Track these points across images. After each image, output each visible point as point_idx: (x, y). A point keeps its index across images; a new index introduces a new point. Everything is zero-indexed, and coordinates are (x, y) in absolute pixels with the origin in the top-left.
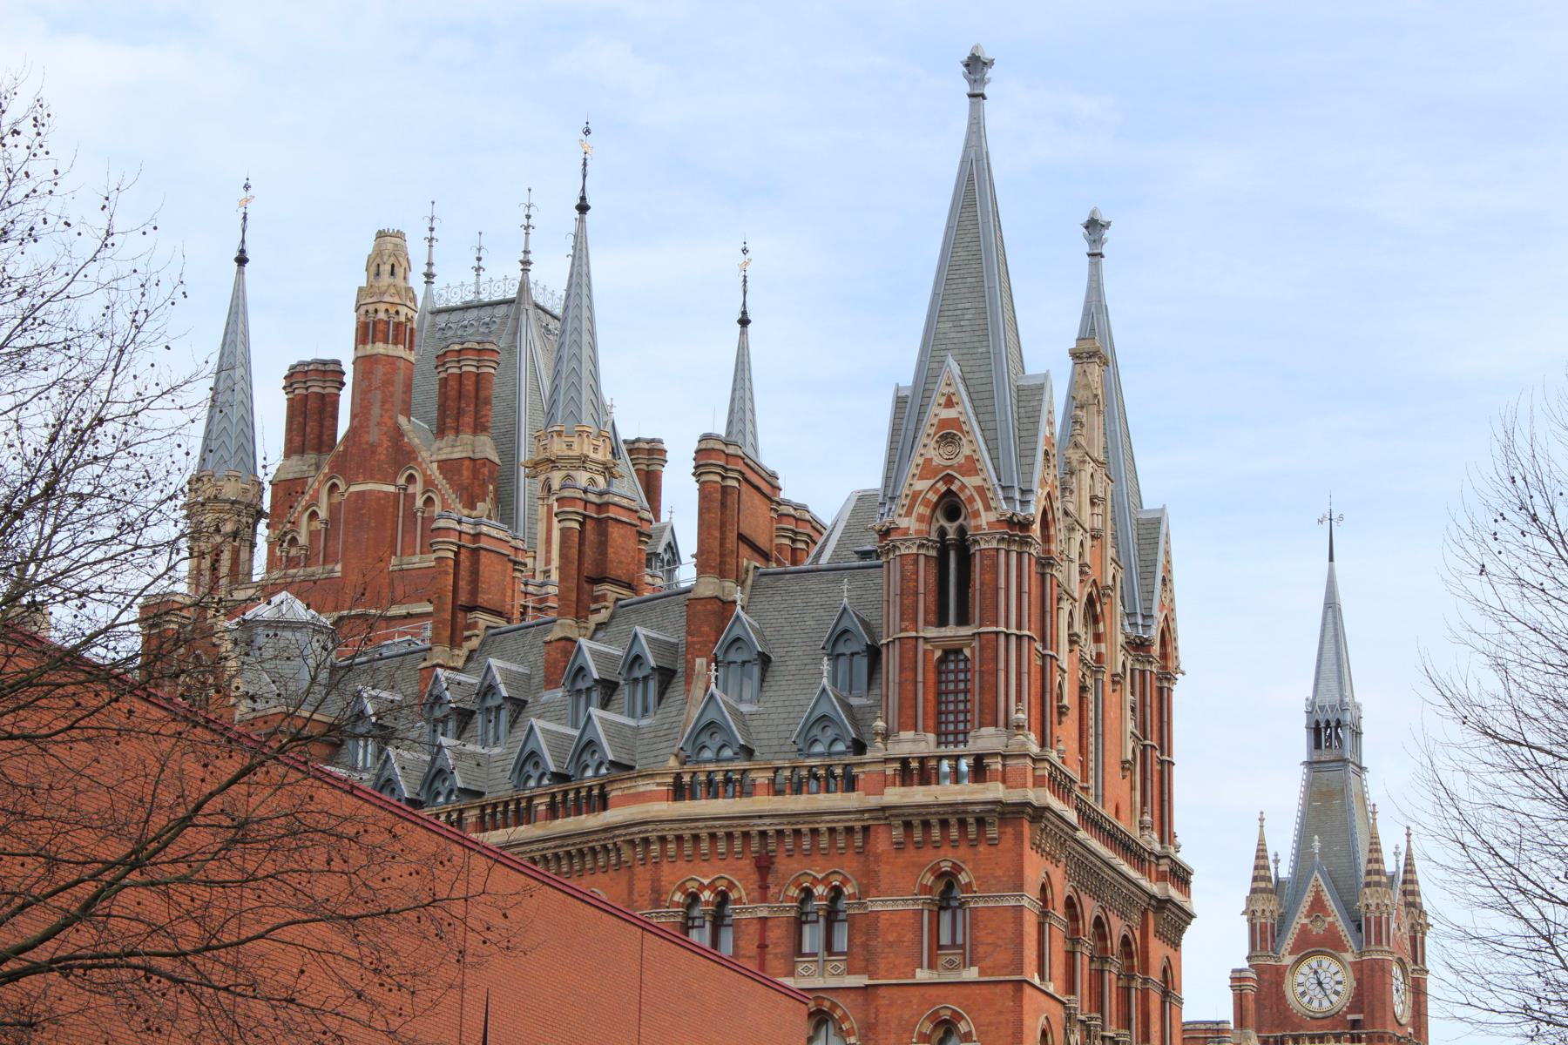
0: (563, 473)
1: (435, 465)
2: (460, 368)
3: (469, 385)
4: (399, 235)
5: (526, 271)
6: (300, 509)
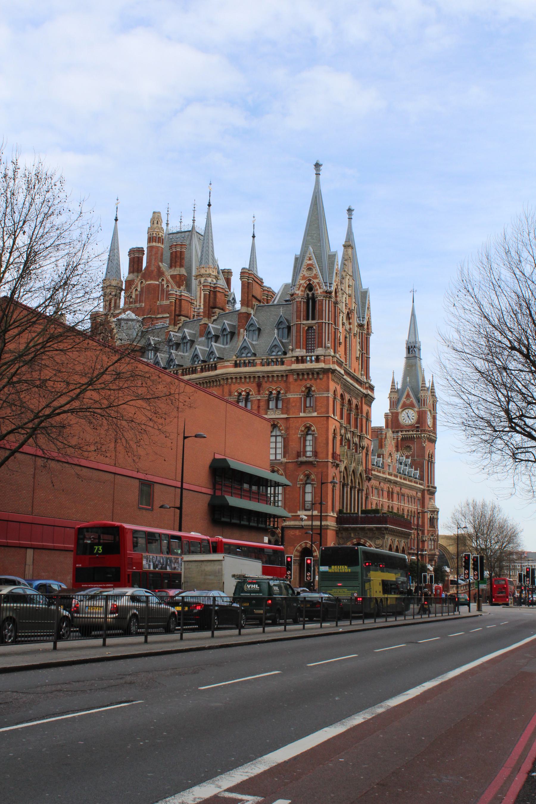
3: (178, 254)
4: (159, 213)
5: (194, 223)
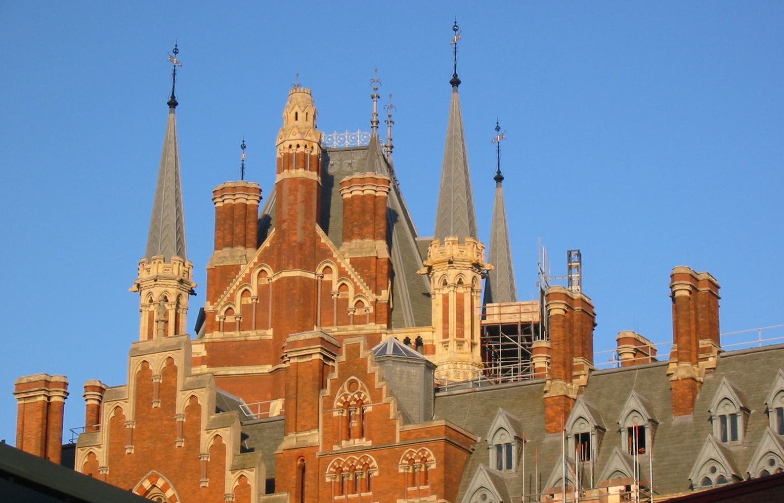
0: (457, 271)
1: (348, 261)
2: (363, 191)
6: (234, 287)
